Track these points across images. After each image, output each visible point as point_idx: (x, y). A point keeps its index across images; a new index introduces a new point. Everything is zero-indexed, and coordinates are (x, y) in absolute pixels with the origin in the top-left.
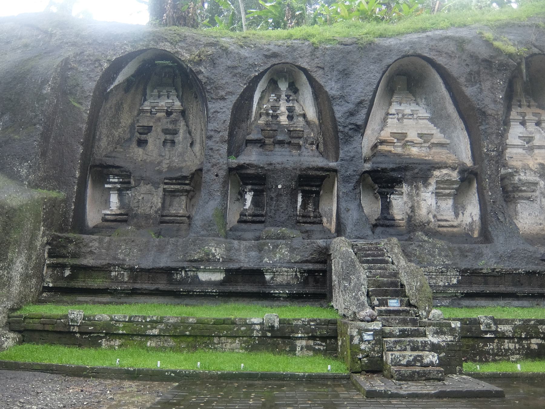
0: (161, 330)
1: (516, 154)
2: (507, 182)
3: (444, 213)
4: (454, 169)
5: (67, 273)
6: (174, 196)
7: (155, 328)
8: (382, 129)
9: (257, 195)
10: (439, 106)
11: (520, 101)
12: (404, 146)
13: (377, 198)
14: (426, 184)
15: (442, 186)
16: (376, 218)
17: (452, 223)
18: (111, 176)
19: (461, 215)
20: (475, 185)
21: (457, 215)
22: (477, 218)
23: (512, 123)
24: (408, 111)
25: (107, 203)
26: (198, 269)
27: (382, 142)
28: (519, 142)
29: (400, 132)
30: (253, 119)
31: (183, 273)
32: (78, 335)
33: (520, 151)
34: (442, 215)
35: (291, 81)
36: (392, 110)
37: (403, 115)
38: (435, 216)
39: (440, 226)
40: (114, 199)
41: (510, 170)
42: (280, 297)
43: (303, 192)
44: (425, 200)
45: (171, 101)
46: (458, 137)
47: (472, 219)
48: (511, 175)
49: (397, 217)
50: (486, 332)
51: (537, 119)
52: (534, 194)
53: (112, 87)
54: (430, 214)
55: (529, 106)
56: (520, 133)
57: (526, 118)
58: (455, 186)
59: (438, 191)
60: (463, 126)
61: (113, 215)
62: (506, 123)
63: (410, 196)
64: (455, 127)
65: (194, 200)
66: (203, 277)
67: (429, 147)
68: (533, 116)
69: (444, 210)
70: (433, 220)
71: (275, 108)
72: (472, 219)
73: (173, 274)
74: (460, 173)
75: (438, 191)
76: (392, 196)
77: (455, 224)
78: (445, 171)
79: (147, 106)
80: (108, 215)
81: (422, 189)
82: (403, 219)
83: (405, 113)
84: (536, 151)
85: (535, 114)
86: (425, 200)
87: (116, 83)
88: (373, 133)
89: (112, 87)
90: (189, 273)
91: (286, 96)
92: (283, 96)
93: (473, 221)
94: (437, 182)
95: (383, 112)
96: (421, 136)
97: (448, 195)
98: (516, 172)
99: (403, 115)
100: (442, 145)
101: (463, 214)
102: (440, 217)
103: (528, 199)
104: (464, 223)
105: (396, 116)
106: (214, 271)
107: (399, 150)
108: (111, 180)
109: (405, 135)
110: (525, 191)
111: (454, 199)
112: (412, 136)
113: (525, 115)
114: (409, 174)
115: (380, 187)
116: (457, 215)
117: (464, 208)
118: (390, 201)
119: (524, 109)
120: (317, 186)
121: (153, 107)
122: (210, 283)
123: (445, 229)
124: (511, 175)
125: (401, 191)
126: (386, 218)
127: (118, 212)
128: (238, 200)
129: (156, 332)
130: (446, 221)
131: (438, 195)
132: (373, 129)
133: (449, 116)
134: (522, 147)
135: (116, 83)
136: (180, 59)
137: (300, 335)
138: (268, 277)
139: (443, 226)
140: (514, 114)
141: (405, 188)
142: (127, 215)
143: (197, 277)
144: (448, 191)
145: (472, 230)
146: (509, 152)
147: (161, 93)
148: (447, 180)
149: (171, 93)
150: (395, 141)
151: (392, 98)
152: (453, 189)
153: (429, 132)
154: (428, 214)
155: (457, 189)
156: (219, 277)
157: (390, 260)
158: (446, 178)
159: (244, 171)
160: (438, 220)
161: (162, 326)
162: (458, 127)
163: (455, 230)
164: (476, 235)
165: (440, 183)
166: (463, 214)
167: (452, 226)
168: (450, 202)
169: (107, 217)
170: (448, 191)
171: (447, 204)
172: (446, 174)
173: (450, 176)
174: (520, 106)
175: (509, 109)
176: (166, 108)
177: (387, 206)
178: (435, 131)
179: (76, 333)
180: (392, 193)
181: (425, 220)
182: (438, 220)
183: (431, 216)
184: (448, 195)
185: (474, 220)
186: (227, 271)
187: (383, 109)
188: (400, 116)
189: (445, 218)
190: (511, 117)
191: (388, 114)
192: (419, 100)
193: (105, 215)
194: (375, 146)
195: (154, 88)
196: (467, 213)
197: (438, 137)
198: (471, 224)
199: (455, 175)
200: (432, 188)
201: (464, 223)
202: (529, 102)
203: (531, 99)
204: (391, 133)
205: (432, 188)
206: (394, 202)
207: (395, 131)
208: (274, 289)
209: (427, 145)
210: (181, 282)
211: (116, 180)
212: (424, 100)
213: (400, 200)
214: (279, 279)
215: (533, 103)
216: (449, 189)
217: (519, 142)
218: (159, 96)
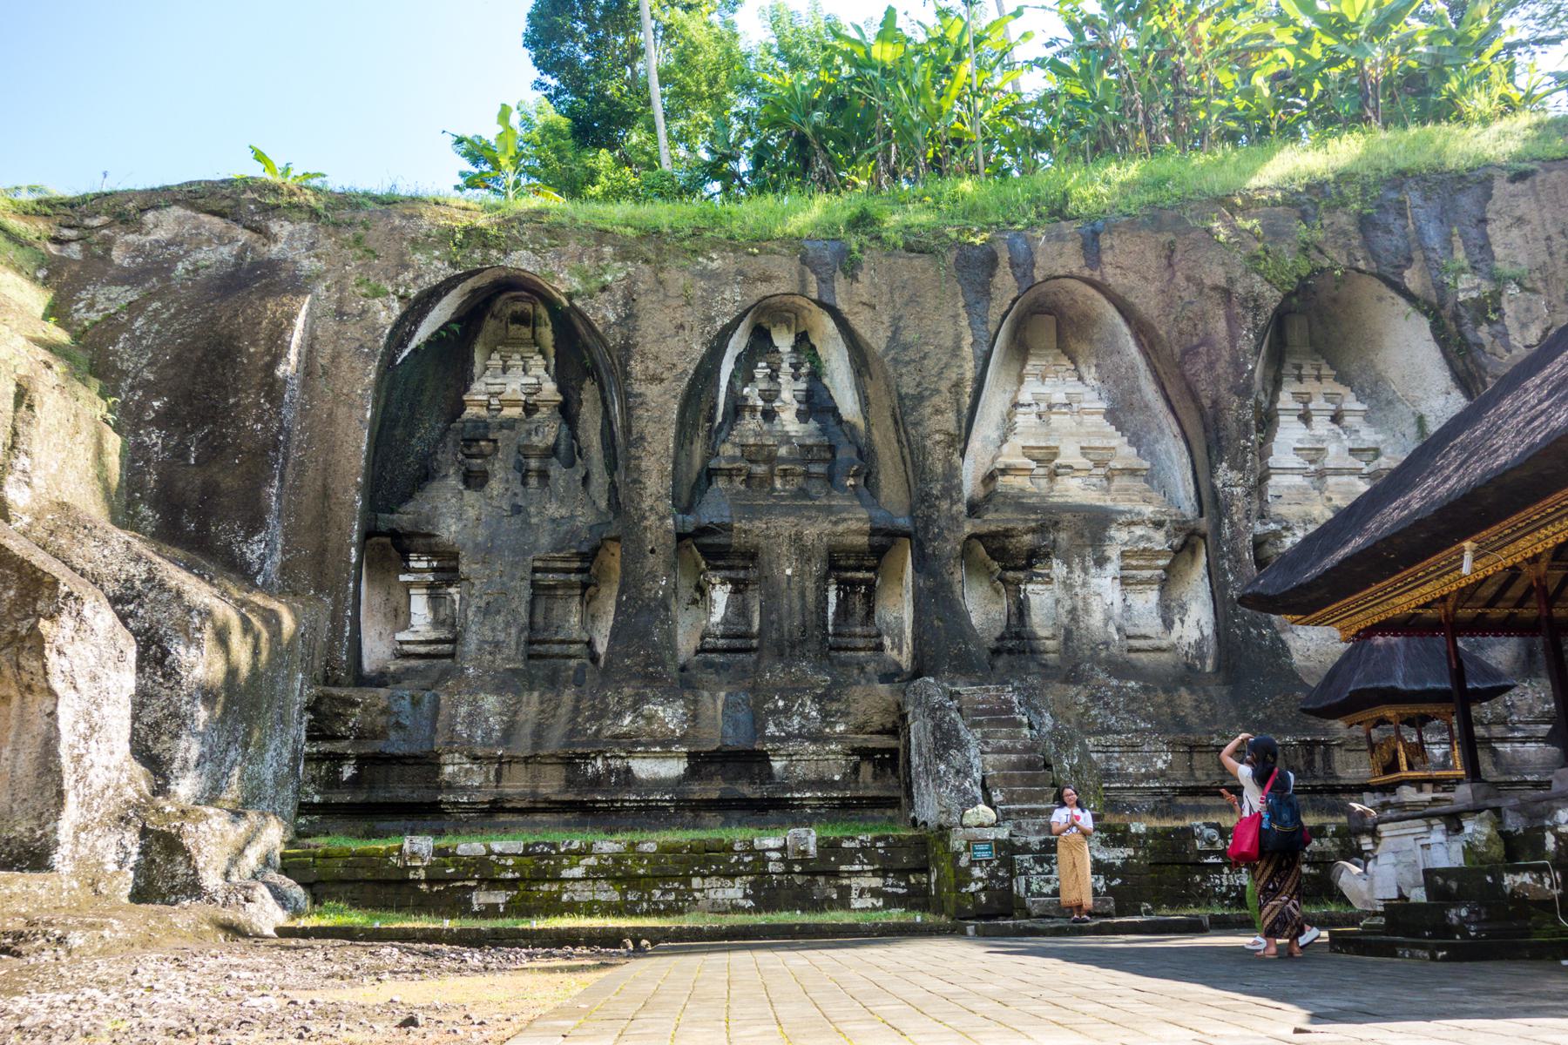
0: (588, 867)
1: (1288, 487)
2: (1269, 550)
3: (1141, 622)
4: (1158, 525)
5: (348, 771)
6: (555, 596)
7: (578, 865)
8: (1004, 440)
9: (739, 587)
10: (1126, 383)
11: (1299, 367)
12: (1053, 475)
13: (998, 592)
14: (1101, 562)
15: (1134, 563)
16: (997, 634)
17: (1156, 643)
18: (413, 556)
19: (1177, 624)
20: (1203, 559)
21: (1168, 624)
22: (1208, 631)
23: (1282, 418)
24: (1058, 397)
25: (400, 617)
26: (630, 754)
27: (1004, 471)
28: (1294, 461)
30: (719, 419)
31: (599, 763)
32: (424, 887)
33: (1298, 480)
35: (802, 329)
36: (1025, 396)
37: (1050, 407)
38: (1119, 630)
39: (1130, 650)
40: (419, 605)
41: (1273, 526)
42: (804, 806)
43: (841, 583)
45: (534, 381)
46: (1168, 452)
48: (1277, 535)
49: (1042, 632)
50: (1207, 854)
51: (1333, 407)
53: (406, 353)
55: (1319, 378)
56: (1299, 441)
57: (1311, 406)
58: (1162, 562)
59: (1125, 573)
60: (1176, 429)
61: (421, 642)
62: (1267, 422)
63: (1068, 586)
64: (1162, 431)
65: (594, 604)
66: (643, 768)
67: (1108, 478)
68: (1327, 400)
69: (1140, 616)
70: (1117, 637)
71: (770, 396)
73: (579, 765)
74: (1168, 536)
75: (1125, 573)
76: (1030, 587)
77: (1164, 644)
78: (1139, 531)
79: (478, 393)
80: (408, 642)
81: (1093, 571)
82: (1054, 637)
83: (1053, 401)
84: (1331, 480)
85: (1329, 398)
87: (412, 345)
88: (985, 447)
89: (406, 353)
90: (612, 762)
91: (791, 365)
92: (785, 366)
93: (1203, 638)
94: (1123, 555)
95: (1007, 397)
96: (1084, 451)
97: (1149, 581)
98: (1287, 529)
99: (1050, 407)
100: (1133, 472)
101: (1182, 621)
102: (1131, 630)
104: (1184, 641)
105: (1034, 408)
106: (666, 755)
108: (412, 564)
109: (1054, 453)
111: (1162, 590)
112: (1069, 454)
113: (1310, 400)
114: (1063, 537)
115: (1005, 569)
116: (1168, 624)
117: (1183, 608)
118: (1026, 597)
119: (1309, 386)
120: (868, 569)
121: (492, 395)
122: (658, 784)
123: (1142, 656)
124: (1277, 535)
125: (1048, 575)
126: (1018, 636)
127: (433, 635)
128: (695, 602)
129: (578, 872)
130: (1145, 637)
131: (1125, 581)
132: (986, 438)
133: (1147, 406)
134: (1305, 474)
135: (412, 345)
136: (557, 290)
137: (857, 868)
138: (778, 765)
139: (1138, 650)
140: (1286, 399)
141: (1058, 569)
142: (453, 641)
143: (629, 770)
144: (1147, 574)
145: (1201, 657)
146: (1276, 482)
147: (510, 363)
148: (1145, 549)
149: (532, 362)
150: (1033, 465)
151: (1023, 367)
152: (1157, 568)
153: (1105, 443)
154: (1106, 625)
155: (1166, 569)
156: (674, 768)
157: (1025, 720)
158: (1142, 545)
159: (707, 540)
160: (1129, 637)
161: (592, 861)
162: (1167, 431)
164: (1209, 665)
166: (1182, 621)
167: (1159, 650)
168: (1153, 596)
169: (406, 647)
170: (1147, 574)
171: (1146, 601)
172: (1142, 536)
173: (1149, 539)
174: (1300, 379)
175: (1277, 384)
176: (523, 398)
177: (1021, 610)
178: (1118, 441)
179: (419, 881)
180: (1030, 581)
181: (1099, 636)
182: (1129, 637)
183: (1112, 629)
184: (1149, 581)
186: (690, 755)
187: (1005, 391)
188: (1043, 406)
189: (1143, 631)
190: (1279, 406)
191: (1016, 405)
192: (1083, 369)
193: (401, 643)
194: (990, 478)
195: (493, 350)
196: (1190, 620)
197: (1125, 454)
198: (1199, 644)
199: (1159, 540)
200: (1112, 568)
201: (1184, 641)
202: (1319, 370)
203: (1323, 362)
205: (1112, 568)
206: (1034, 601)
207: (1032, 443)
208: (791, 791)
209: (1101, 471)
210: (597, 782)
211: (424, 565)
212: (1093, 369)
213: (1047, 594)
214: (799, 770)
215: (1326, 371)
216: (1149, 568)
217: (1294, 461)
218: (505, 370)
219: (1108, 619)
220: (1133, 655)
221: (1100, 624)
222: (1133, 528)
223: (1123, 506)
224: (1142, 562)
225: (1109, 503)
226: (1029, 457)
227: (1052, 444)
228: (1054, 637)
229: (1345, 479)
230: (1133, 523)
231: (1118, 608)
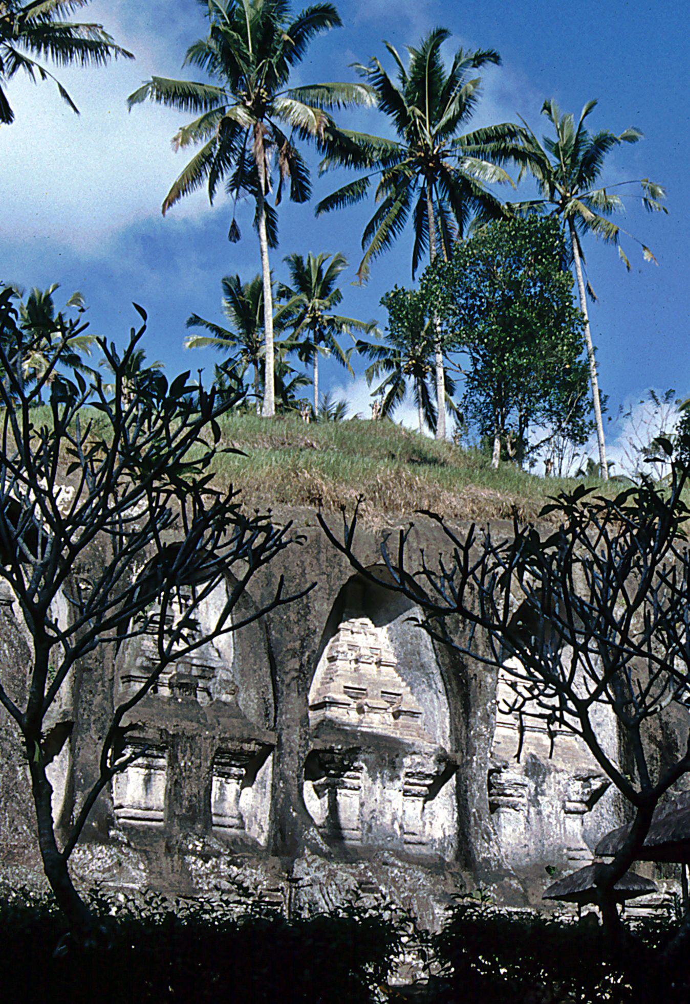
1: (504, 737)
15: (411, 780)
22: (451, 831)
27: (334, 703)
29: (356, 686)
34: (408, 825)
38: (401, 827)
44: (390, 801)
47: (444, 833)
52: (520, 799)
54: (396, 822)
58: (429, 782)
69: (410, 817)
72: (444, 833)
77: (424, 840)
86: (390, 801)
94: (407, 775)
103: (514, 807)
107: (353, 717)
110: (511, 795)
123: (411, 846)
130: (414, 834)
139: (409, 843)
150: (351, 701)
152: (424, 785)
154: (393, 824)
155: (428, 786)
163: (424, 850)
164: (449, 857)
165: (410, 777)
166: (431, 824)
167: (421, 843)
177: (334, 807)
178: (404, 689)
183: (396, 826)
185: (447, 834)
189: (412, 830)
204: (345, 687)
207: (350, 684)
219: (394, 819)
220: (405, 846)
221: (389, 823)
222: (414, 757)
223: (408, 739)
224: (416, 781)
225: (398, 736)
226: (345, 693)
227: (364, 687)
228: (358, 829)
229: (537, 734)
230: (415, 753)
231: (400, 813)
